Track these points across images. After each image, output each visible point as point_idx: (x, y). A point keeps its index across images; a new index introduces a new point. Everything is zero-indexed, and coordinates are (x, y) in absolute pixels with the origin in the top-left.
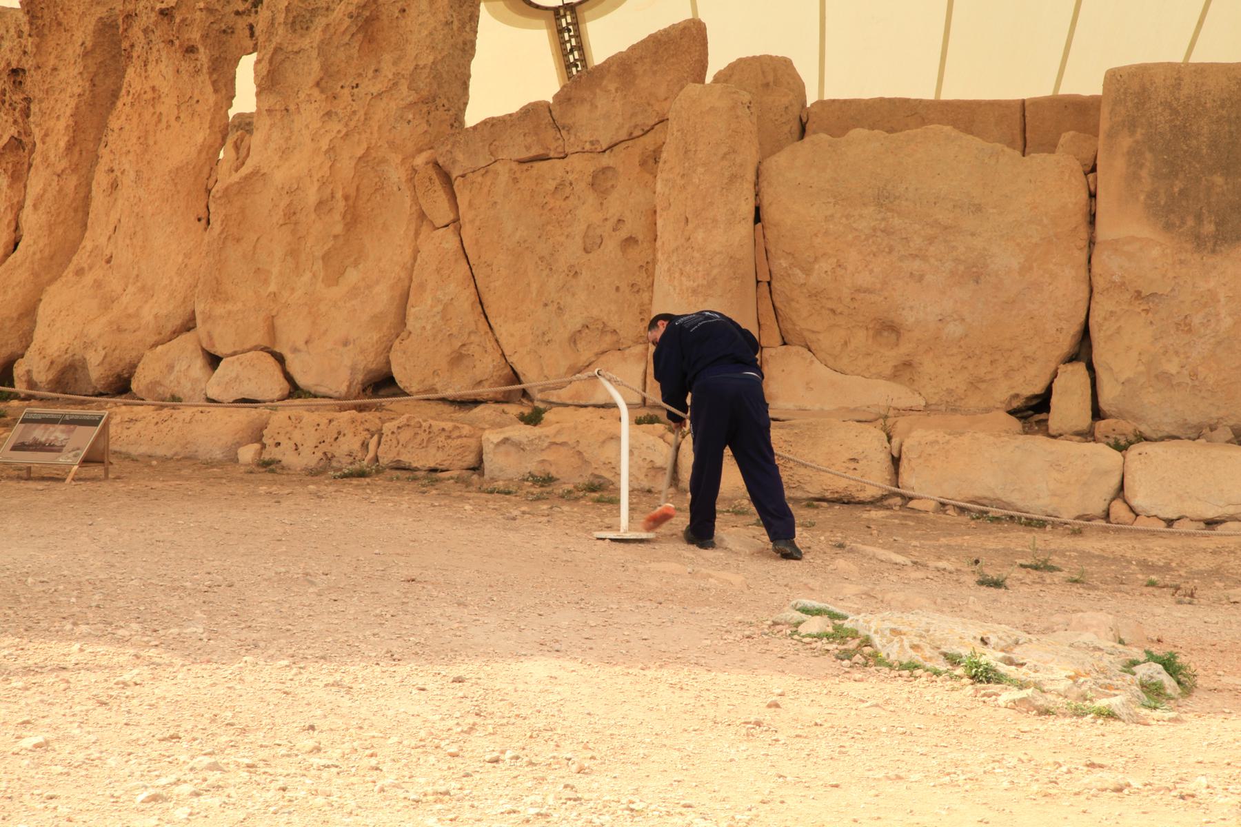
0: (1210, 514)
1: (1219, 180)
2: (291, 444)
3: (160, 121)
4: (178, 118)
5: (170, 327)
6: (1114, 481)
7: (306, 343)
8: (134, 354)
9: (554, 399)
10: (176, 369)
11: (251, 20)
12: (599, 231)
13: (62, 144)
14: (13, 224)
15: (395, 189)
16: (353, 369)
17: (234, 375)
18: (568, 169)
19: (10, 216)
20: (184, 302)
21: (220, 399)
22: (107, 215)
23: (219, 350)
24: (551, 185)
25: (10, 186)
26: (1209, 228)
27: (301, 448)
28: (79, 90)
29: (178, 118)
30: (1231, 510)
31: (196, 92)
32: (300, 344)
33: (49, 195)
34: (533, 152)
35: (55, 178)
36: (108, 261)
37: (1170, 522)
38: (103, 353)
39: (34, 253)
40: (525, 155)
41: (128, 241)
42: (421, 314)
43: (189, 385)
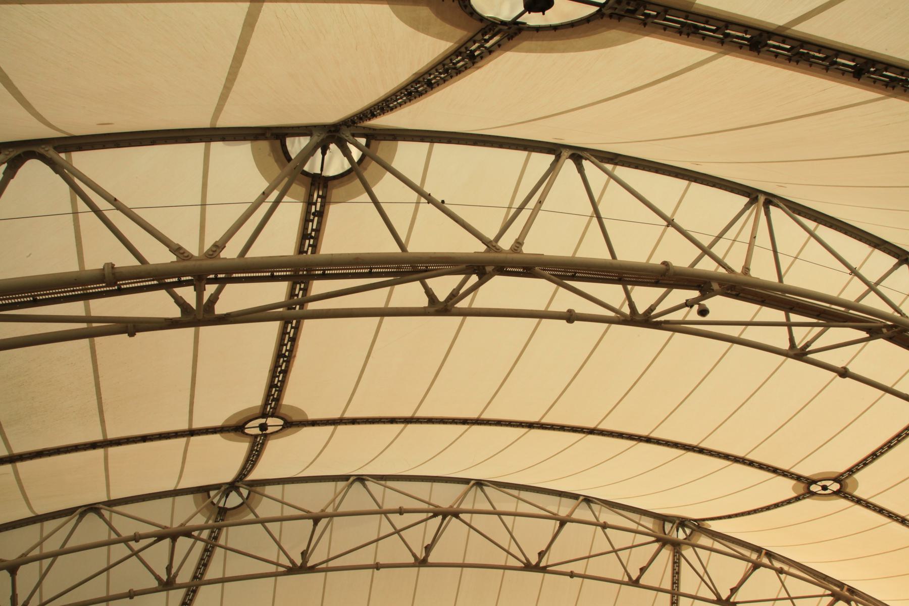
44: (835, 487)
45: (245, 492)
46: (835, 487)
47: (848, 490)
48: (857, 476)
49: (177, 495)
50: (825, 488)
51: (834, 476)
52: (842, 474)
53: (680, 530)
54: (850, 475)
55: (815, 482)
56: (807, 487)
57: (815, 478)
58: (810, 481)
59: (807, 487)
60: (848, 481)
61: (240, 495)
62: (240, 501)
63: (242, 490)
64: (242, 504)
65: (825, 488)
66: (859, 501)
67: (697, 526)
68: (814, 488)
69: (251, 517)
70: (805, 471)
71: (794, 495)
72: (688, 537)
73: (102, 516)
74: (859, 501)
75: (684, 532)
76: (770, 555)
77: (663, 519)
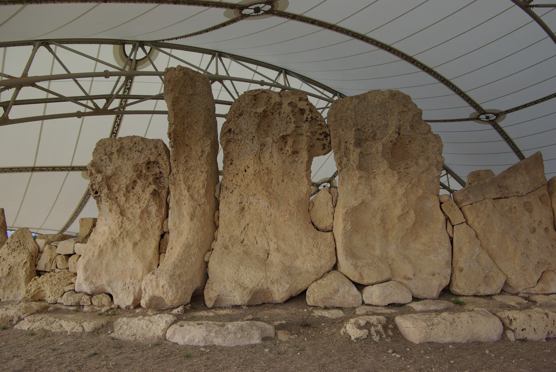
2: (532, 328)
3: (271, 182)
4: (283, 181)
5: (323, 271)
7: (414, 275)
8: (304, 285)
9: (533, 292)
10: (340, 292)
11: (325, 142)
12: (532, 226)
13: (203, 191)
14: (161, 227)
15: (429, 209)
16: (440, 285)
17: (389, 292)
18: (513, 202)
19: (159, 223)
20: (330, 260)
21: (380, 304)
22: (239, 222)
23: (365, 282)
24: (507, 208)
25: (157, 211)
27: (537, 330)
28: (206, 169)
29: (283, 181)
31: (292, 170)
32: (410, 275)
33: (197, 213)
34: (499, 196)
35: (198, 207)
36: (242, 242)
38: (288, 286)
39: (198, 240)
40: (496, 197)
41: (262, 233)
42: (461, 261)
43: (351, 298)
44: (493, 117)
45: (148, 48)
46: (493, 117)
48: (507, 115)
49: (102, 43)
50: (487, 118)
51: (497, 112)
52: (501, 113)
54: (505, 114)
56: (480, 114)
58: (484, 113)
61: (144, 50)
62: (144, 55)
63: (146, 47)
64: (145, 57)
65: (487, 118)
68: (483, 117)
69: (150, 68)
70: (485, 107)
73: (50, 50)
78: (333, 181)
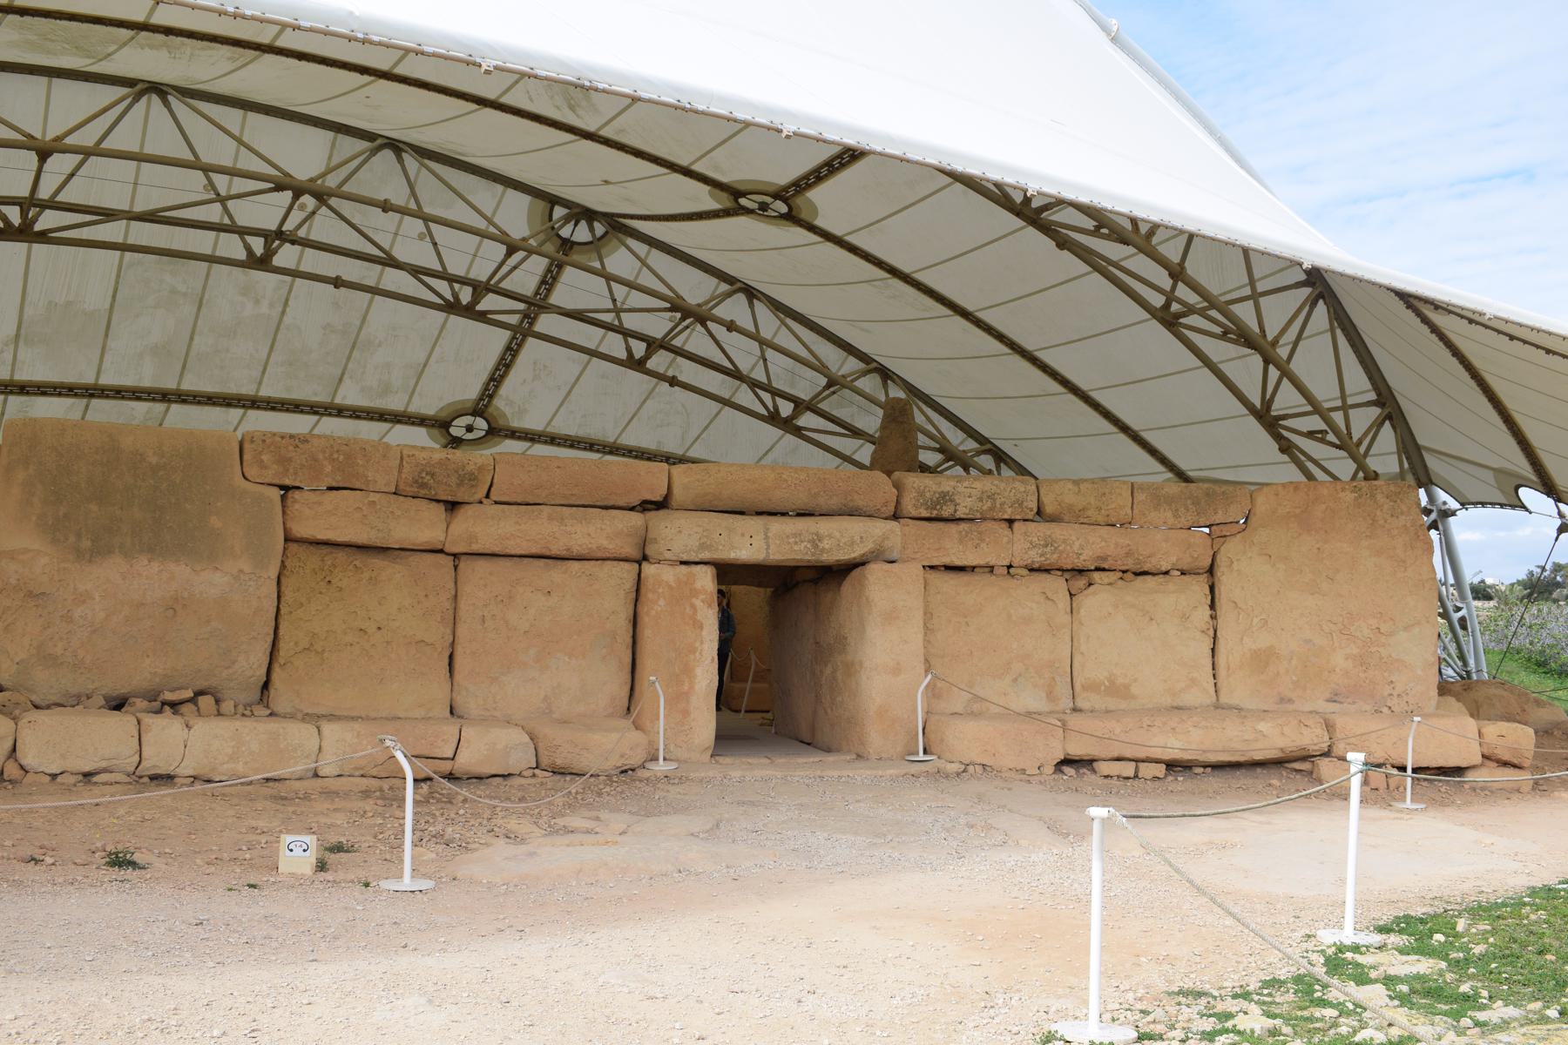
0: (87, 769)
1: (94, 507)
6: (8, 745)
26: (86, 544)
30: (104, 764)
37: (54, 776)
44: (782, 208)
46: (782, 208)
47: (804, 215)
51: (771, 189)
52: (786, 189)
53: (583, 224)
55: (744, 194)
56: (735, 199)
57: (742, 187)
58: (735, 193)
59: (735, 199)
60: (799, 201)
66: (827, 236)
67: (617, 226)
68: (743, 201)
71: (716, 206)
72: (596, 244)
74: (827, 236)
75: (592, 229)
76: (751, 293)
77: (553, 200)
78: (490, 410)
